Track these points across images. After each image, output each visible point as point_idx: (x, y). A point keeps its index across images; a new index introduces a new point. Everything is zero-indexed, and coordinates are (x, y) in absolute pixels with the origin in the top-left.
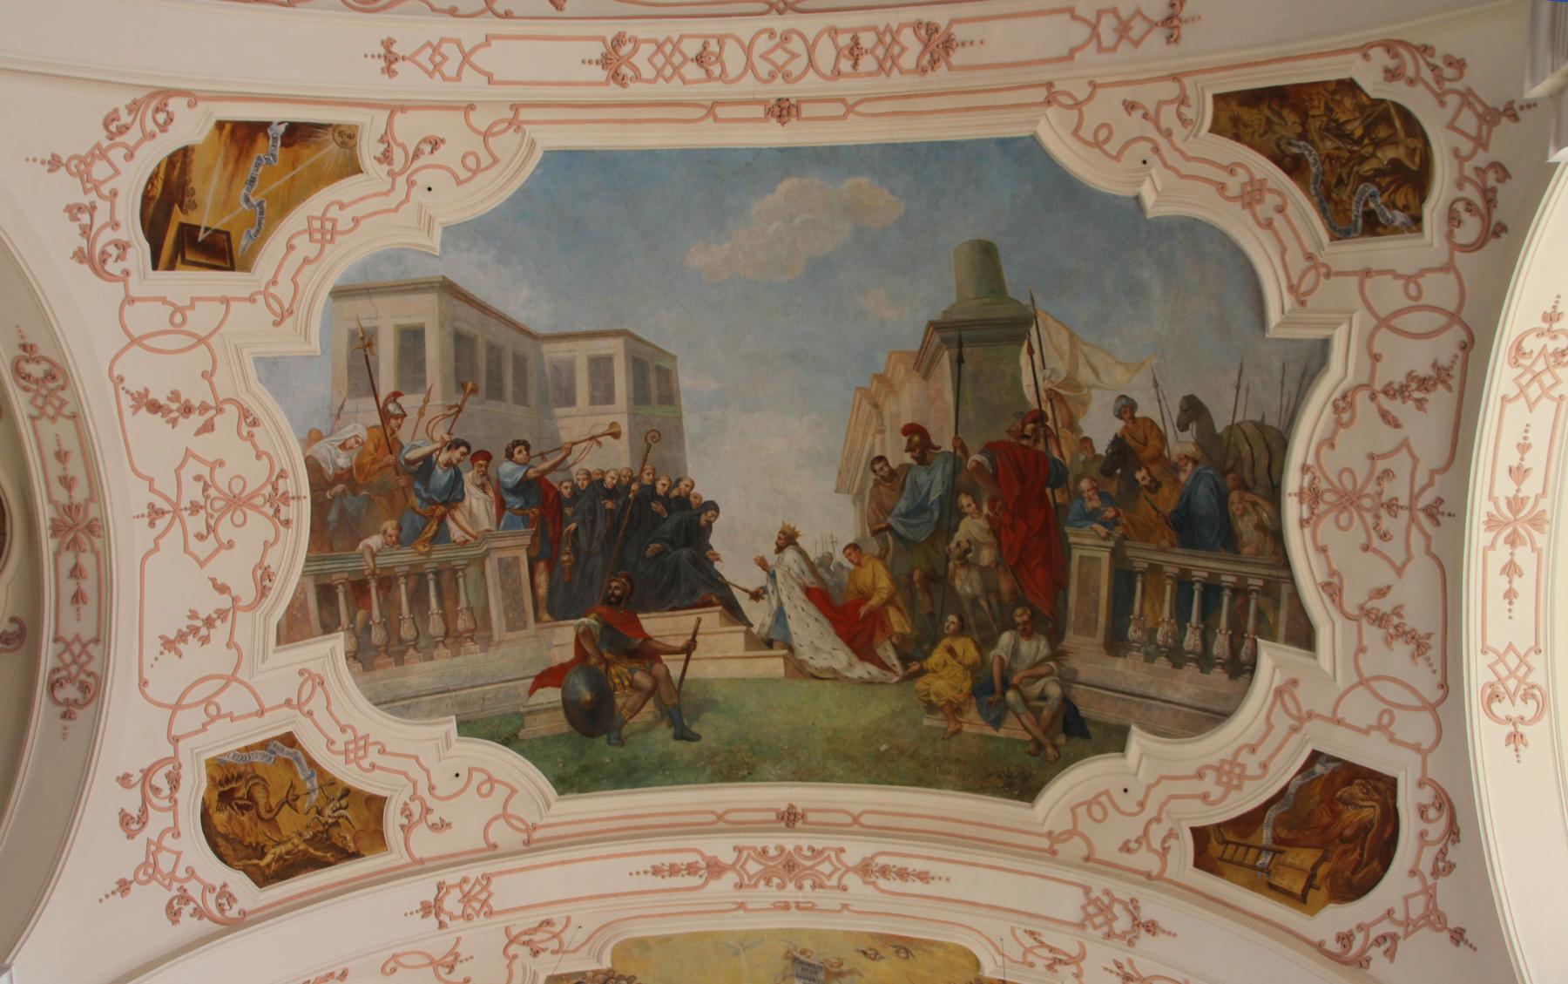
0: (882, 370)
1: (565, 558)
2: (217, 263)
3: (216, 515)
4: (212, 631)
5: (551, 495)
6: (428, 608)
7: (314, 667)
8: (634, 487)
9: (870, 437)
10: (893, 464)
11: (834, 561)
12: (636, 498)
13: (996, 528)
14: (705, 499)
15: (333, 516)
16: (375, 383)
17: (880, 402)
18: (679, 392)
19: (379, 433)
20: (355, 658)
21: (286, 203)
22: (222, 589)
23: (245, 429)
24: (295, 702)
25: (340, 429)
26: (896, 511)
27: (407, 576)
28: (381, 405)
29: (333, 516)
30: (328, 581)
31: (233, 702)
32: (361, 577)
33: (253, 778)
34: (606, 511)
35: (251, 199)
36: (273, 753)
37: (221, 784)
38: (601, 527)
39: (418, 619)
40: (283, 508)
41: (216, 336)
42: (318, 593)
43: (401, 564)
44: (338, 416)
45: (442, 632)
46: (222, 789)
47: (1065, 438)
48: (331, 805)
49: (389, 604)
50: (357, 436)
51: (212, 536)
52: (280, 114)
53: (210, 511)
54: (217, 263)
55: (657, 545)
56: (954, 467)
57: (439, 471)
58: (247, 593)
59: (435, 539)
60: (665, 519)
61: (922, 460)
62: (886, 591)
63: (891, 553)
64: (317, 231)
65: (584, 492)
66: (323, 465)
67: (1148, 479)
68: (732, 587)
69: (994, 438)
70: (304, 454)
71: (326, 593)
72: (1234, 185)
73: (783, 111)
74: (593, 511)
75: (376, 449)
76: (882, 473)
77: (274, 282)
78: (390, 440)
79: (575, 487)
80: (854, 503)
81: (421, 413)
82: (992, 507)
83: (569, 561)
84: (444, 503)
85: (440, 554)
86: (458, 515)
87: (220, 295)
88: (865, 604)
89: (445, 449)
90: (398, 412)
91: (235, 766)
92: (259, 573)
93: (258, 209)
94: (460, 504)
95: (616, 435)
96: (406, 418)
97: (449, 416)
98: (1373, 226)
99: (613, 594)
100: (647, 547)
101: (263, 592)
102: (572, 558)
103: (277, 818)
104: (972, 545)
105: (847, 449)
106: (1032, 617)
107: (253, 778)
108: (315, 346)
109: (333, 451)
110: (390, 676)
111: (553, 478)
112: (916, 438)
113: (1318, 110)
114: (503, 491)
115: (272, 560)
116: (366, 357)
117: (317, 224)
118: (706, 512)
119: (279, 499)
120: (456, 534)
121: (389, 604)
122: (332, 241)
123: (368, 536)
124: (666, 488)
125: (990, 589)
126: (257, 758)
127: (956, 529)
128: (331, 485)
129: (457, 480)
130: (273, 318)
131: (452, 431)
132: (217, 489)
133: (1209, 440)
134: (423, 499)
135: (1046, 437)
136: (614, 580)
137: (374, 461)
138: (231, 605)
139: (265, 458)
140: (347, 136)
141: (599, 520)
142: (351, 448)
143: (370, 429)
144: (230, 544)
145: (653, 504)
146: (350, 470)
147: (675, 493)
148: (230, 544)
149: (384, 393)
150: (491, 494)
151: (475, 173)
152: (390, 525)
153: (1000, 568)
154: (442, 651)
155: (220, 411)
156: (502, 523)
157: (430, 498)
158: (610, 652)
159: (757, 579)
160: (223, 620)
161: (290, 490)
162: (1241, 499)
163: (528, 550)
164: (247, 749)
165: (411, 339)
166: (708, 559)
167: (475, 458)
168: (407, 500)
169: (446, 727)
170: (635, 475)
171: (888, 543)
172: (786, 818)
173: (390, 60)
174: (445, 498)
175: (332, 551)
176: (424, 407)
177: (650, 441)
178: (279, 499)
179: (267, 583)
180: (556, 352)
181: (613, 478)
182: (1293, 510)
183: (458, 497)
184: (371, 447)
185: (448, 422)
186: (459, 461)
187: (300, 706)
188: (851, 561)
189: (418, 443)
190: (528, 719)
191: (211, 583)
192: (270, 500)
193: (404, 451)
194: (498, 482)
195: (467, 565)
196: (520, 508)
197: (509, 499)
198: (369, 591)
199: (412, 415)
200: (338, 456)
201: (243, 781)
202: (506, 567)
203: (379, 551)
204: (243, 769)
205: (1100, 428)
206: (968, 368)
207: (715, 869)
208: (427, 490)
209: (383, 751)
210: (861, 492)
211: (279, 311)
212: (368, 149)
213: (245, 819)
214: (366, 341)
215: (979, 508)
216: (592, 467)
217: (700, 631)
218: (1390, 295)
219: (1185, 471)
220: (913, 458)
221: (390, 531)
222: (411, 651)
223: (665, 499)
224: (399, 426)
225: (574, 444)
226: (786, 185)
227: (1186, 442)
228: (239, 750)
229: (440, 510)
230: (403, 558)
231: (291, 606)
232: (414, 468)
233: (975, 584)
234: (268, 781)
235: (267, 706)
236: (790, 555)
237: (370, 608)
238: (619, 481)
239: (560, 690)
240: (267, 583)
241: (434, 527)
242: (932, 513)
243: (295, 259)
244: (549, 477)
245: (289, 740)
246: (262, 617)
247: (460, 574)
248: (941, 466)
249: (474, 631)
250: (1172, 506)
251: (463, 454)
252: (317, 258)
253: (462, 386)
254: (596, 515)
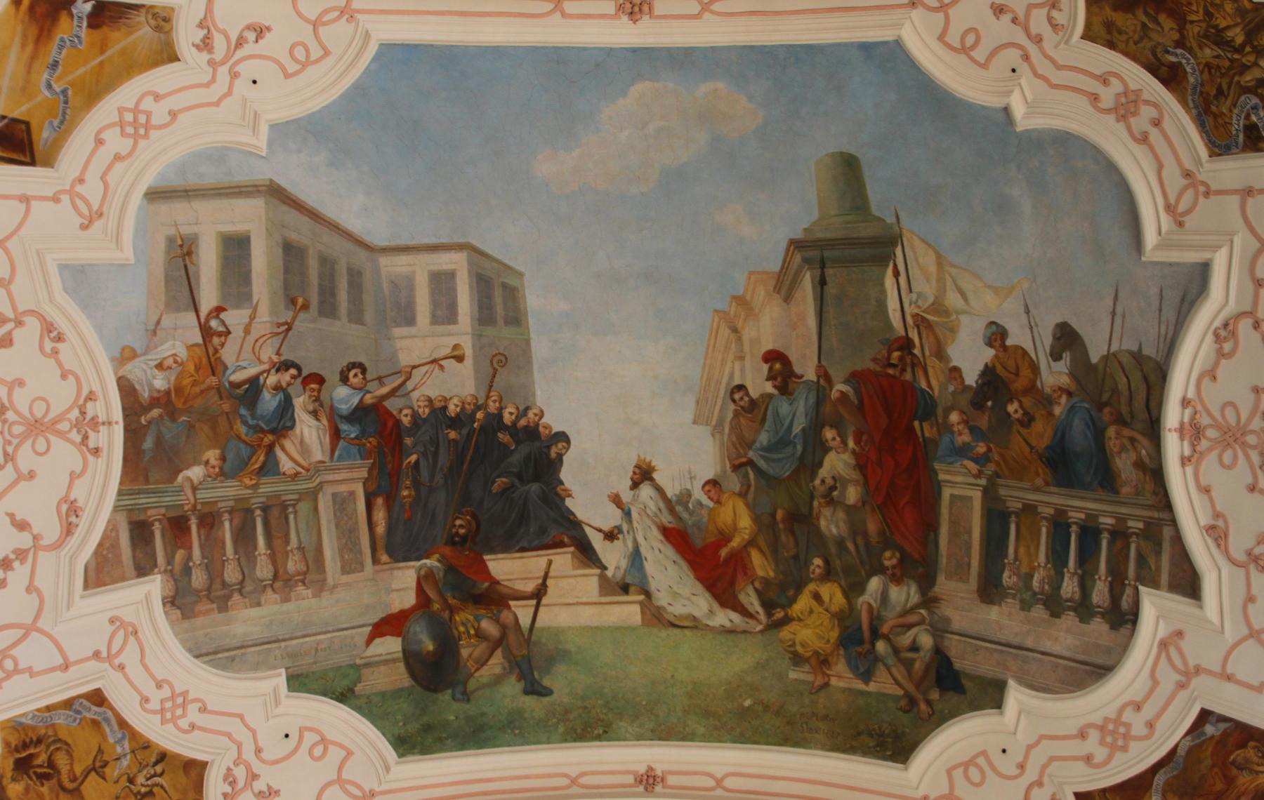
0: (741, 293)
1: (405, 493)
2: (14, 156)
3: (15, 441)
4: (10, 574)
5: (390, 424)
6: (255, 548)
7: (128, 615)
8: (479, 415)
9: (729, 365)
10: (754, 393)
11: (693, 498)
12: (481, 427)
13: (862, 464)
14: (556, 428)
15: (148, 444)
16: (196, 296)
17: (739, 329)
18: (526, 312)
19: (200, 352)
20: (173, 603)
21: (94, 92)
22: (22, 526)
23: (48, 345)
24: (104, 654)
25: (156, 348)
26: (757, 445)
27: (231, 512)
28: (203, 320)
29: (148, 444)
30: (142, 517)
31: (34, 653)
32: (180, 513)
33: (55, 742)
34: (449, 441)
35: (54, 86)
36: (78, 712)
37: (17, 750)
38: (444, 459)
39: (243, 560)
40: (92, 435)
41: (15, 238)
42: (131, 531)
43: (225, 499)
44: (155, 333)
45: (270, 575)
46: (18, 756)
47: (933, 367)
48: (145, 772)
49: (212, 545)
50: (175, 355)
51: (10, 465)
53: (8, 437)
54: (14, 156)
55: (504, 480)
56: (818, 396)
57: (266, 395)
58: (50, 529)
59: (263, 471)
60: (512, 452)
61: (784, 389)
62: (747, 531)
63: (752, 489)
64: (130, 124)
65: (425, 420)
66: (137, 387)
67: (1021, 412)
68: (584, 526)
69: (859, 367)
70: (116, 374)
71: (140, 531)
74: (435, 442)
75: (197, 369)
76: (742, 403)
77: (81, 180)
78: (212, 359)
79: (415, 415)
80: (713, 435)
81: (247, 331)
82: (857, 442)
83: (409, 496)
84: (273, 431)
85: (268, 487)
86: (288, 444)
87: (19, 193)
88: (725, 545)
89: (273, 371)
90: (221, 329)
91: (34, 728)
92: (65, 507)
93: (62, 97)
94: (290, 432)
95: (460, 359)
96: (231, 336)
97: (278, 334)
99: (457, 533)
100: (494, 482)
101: (69, 530)
102: (413, 493)
103: (82, 788)
104: (837, 482)
105: (705, 376)
106: (902, 561)
107: (55, 742)
108: (128, 254)
109: (149, 372)
110: (211, 624)
111: (392, 405)
112: (778, 366)
114: (337, 418)
115: (78, 493)
116: (186, 267)
117: (129, 117)
118: (556, 444)
119: (87, 424)
120: (286, 465)
121: (212, 545)
122: (146, 136)
123: (188, 467)
124: (513, 417)
125: (857, 530)
126: (60, 719)
127: (820, 464)
128: (146, 409)
129: (286, 406)
130: (81, 220)
131: (281, 351)
132: (17, 413)
133: (1084, 371)
134: (249, 427)
135: (913, 366)
136: (458, 518)
137: (195, 383)
138: (32, 544)
139: (71, 379)
141: (441, 451)
142: (169, 368)
143: (190, 347)
144: (31, 475)
145: (500, 435)
146: (168, 393)
147: (523, 422)
148: (31, 475)
149: (204, 310)
150: (325, 421)
152: (212, 455)
153: (868, 508)
154: (270, 595)
155: (19, 323)
156: (337, 453)
157: (257, 425)
158: (454, 598)
159: (609, 517)
160: (23, 561)
161: (99, 415)
162: (1119, 435)
163: (364, 483)
164: (49, 708)
166: (557, 494)
167: (307, 381)
168: (231, 428)
169: (274, 682)
170: (480, 403)
171: (749, 480)
172: (645, 781)
174: (274, 425)
175: (147, 482)
176: (249, 324)
177: (495, 365)
178: (87, 424)
179: (73, 519)
181: (457, 406)
183: (289, 424)
184: (191, 368)
185: (276, 342)
186: (289, 384)
187: (110, 658)
188: (711, 499)
189: (243, 364)
190: (365, 671)
191: (8, 520)
192: (77, 425)
193: (228, 372)
194: (332, 407)
195: (298, 500)
196: (356, 438)
197: (344, 427)
198: (188, 529)
199: (237, 333)
200: (154, 378)
201: (43, 747)
202: (342, 503)
203: (200, 483)
204: (42, 732)
208: (253, 416)
209: (203, 710)
210: (720, 424)
211: (87, 214)
213: (45, 790)
214: (185, 250)
215: (844, 442)
216: (434, 393)
217: (550, 574)
219: (1059, 404)
220: (775, 387)
221: (213, 462)
222: (236, 596)
223: (513, 429)
224: (223, 345)
225: (414, 367)
227: (1060, 373)
228: (38, 710)
229: (269, 438)
230: (228, 492)
231: (100, 545)
232: (240, 391)
233: (842, 524)
234: (72, 746)
235: (72, 659)
237: (190, 548)
238: (463, 408)
239: (399, 640)
240: (73, 519)
241: (262, 458)
242: (795, 447)
243: (105, 155)
244: (387, 404)
245: (98, 698)
246: (67, 560)
247: (291, 510)
248: (805, 395)
249: (305, 573)
250: (1045, 442)
251: (294, 377)
252: (130, 154)
253: (293, 302)
254: (437, 447)
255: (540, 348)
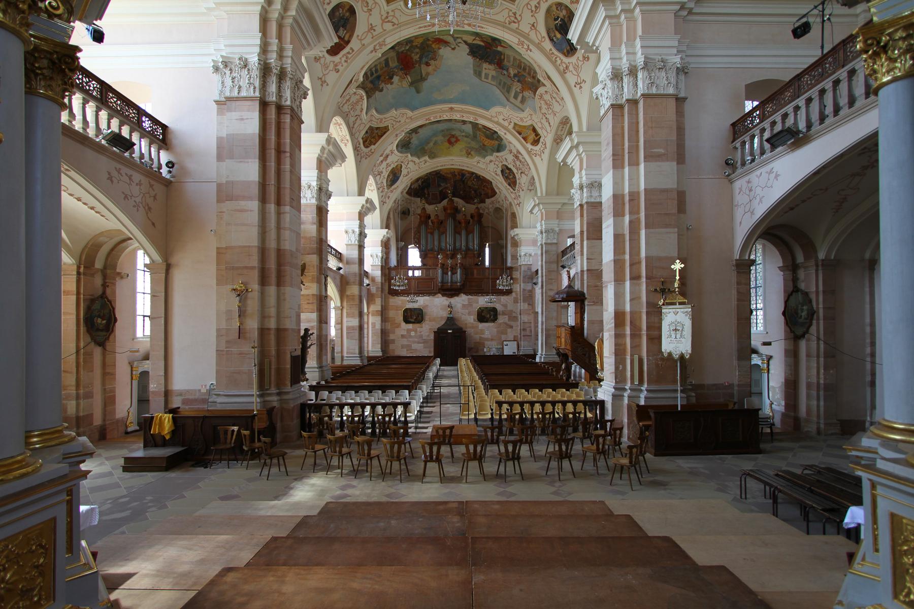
13: (412, 58)
52: (520, 137)
72: (384, 120)
73: (451, 108)
98: (367, 132)
113: (377, 138)
140: (514, 128)
151: (499, 112)
165: (516, 97)
173: (505, 134)
178: (541, 96)
180: (492, 83)
182: (364, 94)
205: (396, 79)
206: (420, 76)
207: (469, 25)
212: (512, 125)
218: (362, 126)
223: (477, 58)
226: (452, 97)
236: (453, 47)
255: (471, 66)
